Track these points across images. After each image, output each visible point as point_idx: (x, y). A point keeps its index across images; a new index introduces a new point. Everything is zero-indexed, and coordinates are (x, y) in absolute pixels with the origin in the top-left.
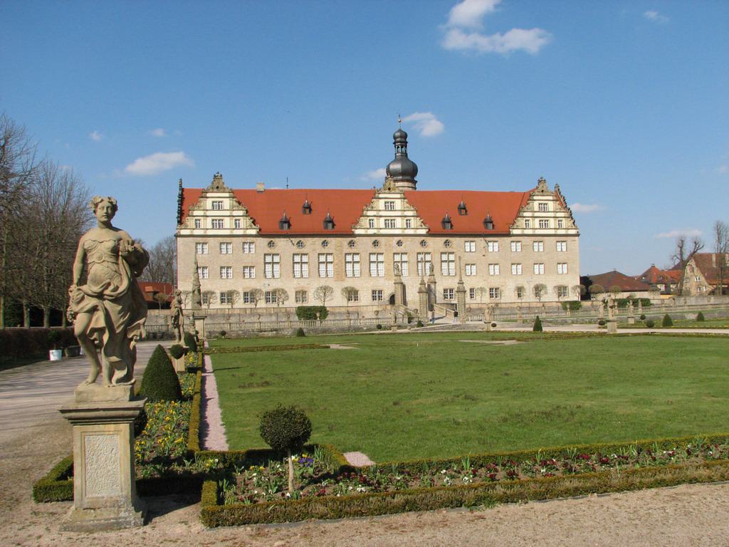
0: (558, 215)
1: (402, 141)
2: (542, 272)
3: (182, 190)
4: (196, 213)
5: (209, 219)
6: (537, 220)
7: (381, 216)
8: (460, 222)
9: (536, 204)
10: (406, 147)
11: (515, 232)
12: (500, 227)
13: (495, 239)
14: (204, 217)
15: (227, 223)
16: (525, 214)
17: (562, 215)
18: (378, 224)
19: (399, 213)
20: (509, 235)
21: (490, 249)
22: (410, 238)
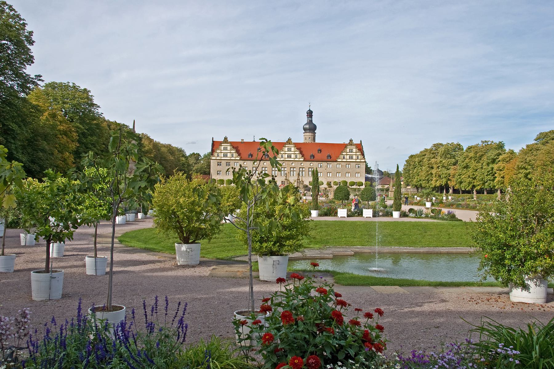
0: (357, 154)
1: (310, 114)
2: (349, 176)
3: (213, 142)
4: (218, 151)
5: (222, 154)
6: (348, 156)
7: (286, 154)
8: (318, 156)
9: (348, 149)
10: (312, 118)
11: (339, 160)
12: (333, 159)
13: (330, 163)
14: (220, 153)
15: (229, 155)
16: (343, 153)
17: (359, 154)
18: (285, 156)
19: (293, 153)
20: (336, 161)
21: (329, 167)
22: (297, 162)
